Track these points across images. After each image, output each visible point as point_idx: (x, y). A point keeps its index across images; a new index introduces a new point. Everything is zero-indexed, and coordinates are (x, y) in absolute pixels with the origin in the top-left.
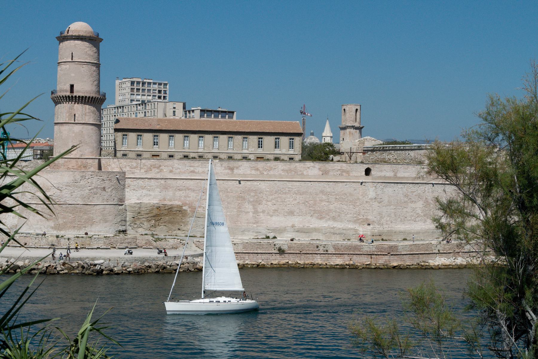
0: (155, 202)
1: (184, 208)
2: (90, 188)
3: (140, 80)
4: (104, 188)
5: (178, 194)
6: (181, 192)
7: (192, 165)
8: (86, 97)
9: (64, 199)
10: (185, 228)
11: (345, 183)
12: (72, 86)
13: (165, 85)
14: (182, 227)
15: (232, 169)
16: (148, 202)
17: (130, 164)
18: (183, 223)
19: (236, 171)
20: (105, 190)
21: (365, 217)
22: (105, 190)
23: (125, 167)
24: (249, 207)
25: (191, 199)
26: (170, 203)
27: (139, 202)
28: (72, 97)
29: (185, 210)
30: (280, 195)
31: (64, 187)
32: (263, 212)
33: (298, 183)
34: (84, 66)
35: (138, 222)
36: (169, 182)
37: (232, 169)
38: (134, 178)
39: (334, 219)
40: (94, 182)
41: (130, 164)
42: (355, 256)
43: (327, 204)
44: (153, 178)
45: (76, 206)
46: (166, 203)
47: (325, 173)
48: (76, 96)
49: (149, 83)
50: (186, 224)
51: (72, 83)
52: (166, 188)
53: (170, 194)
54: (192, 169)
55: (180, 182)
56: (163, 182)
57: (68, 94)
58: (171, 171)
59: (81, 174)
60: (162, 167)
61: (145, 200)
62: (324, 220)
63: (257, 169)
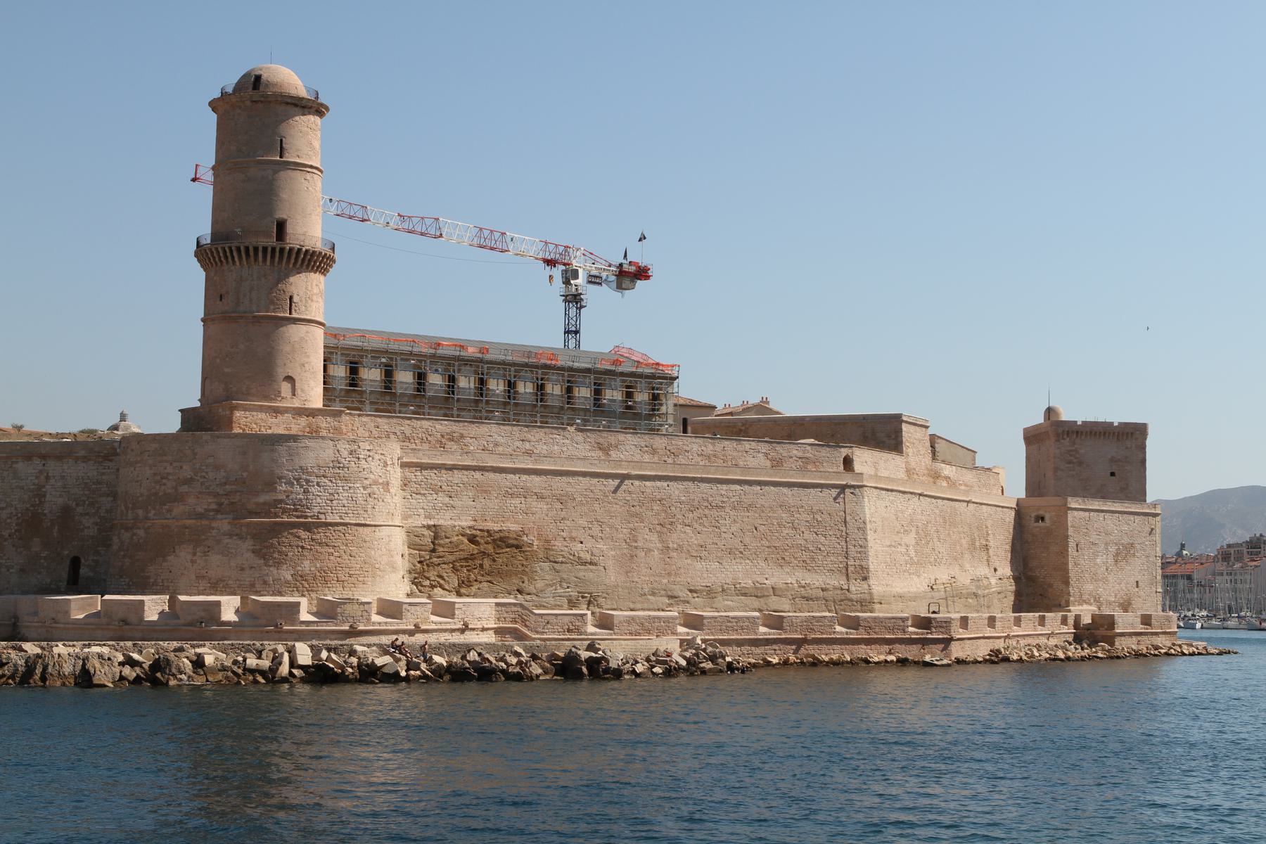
0: (465, 524)
2: (367, 482)
7: (529, 436)
9: (316, 510)
17: (398, 429)
19: (614, 454)
21: (857, 563)
24: (649, 539)
26: (496, 527)
32: (680, 548)
35: (432, 574)
37: (605, 449)
39: (806, 566)
41: (398, 429)
43: (792, 532)
47: (777, 463)
48: (291, 250)
52: (483, 490)
53: (493, 504)
54: (527, 446)
57: (272, 242)
61: (444, 520)
63: (654, 452)
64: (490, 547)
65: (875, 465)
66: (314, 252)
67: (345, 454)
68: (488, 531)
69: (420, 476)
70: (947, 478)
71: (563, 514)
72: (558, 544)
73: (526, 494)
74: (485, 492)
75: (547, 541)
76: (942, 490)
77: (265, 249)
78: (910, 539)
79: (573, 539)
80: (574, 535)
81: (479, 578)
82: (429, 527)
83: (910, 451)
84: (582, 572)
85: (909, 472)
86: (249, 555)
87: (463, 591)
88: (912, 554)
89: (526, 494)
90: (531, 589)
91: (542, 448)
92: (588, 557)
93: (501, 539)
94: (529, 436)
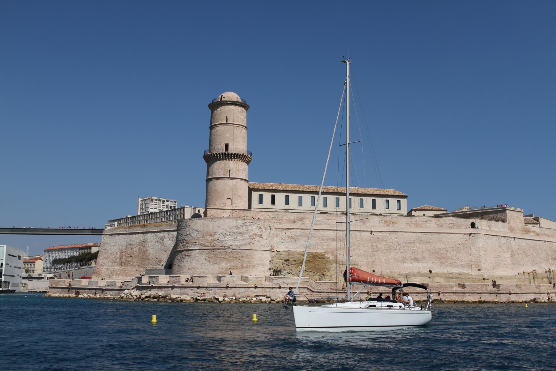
0: (301, 250)
1: (326, 255)
2: (251, 234)
4: (261, 235)
5: (321, 243)
6: (324, 241)
9: (229, 244)
11: (458, 235)
12: (227, 146)
13: (175, 202)
15: (364, 223)
16: (295, 250)
21: (476, 263)
23: (272, 219)
25: (332, 247)
27: (287, 250)
29: (328, 258)
30: (407, 245)
31: (228, 233)
33: (420, 235)
34: (237, 128)
40: (254, 229)
42: (483, 294)
43: (445, 252)
44: (298, 229)
48: (232, 154)
49: (163, 201)
50: (329, 270)
51: (227, 143)
53: (313, 242)
54: (330, 221)
55: (322, 233)
56: (307, 232)
57: (224, 151)
59: (243, 222)
60: (305, 220)
61: (293, 249)
62: (444, 266)
65: (490, 226)
66: (238, 154)
67: (240, 224)
69: (283, 232)
70: (534, 232)
73: (328, 238)
76: (531, 236)
77: (222, 154)
78: (508, 255)
83: (512, 221)
85: (511, 230)
86: (204, 260)
88: (509, 261)
90: (328, 274)
93: (316, 256)
94: (330, 218)
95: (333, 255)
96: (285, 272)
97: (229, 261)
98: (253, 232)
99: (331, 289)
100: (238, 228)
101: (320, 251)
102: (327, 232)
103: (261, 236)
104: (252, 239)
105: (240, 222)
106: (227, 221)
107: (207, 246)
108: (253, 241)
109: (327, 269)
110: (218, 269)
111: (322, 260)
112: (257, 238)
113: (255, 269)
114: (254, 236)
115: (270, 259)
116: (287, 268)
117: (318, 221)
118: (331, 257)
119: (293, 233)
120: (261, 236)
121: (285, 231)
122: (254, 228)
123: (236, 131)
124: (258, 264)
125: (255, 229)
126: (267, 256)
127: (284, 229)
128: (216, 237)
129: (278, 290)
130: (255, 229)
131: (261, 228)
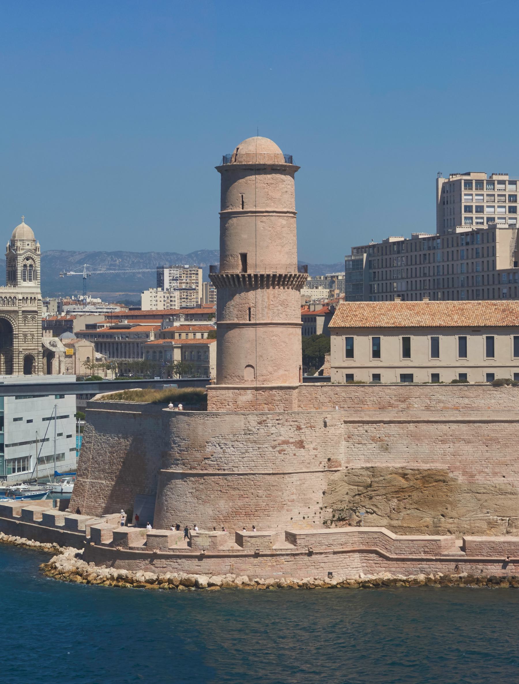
0: (398, 465)
1: (451, 475)
2: (276, 443)
3: (483, 177)
5: (440, 448)
6: (447, 445)
8: (268, 276)
9: (231, 465)
10: (454, 514)
14: (450, 512)
16: (384, 465)
17: (353, 395)
18: (451, 503)
20: (304, 447)
22: (304, 447)
25: (464, 458)
27: (369, 465)
28: (243, 276)
29: (454, 480)
31: (230, 444)
36: (424, 427)
38: (359, 422)
40: (282, 433)
45: (251, 477)
46: (415, 465)
48: (249, 275)
50: (454, 504)
51: (244, 251)
52: (416, 437)
53: (425, 448)
54: (466, 401)
56: (411, 426)
58: (428, 408)
60: (412, 400)
64: (418, 482)
67: (254, 423)
68: (418, 470)
69: (362, 429)
71: (487, 455)
72: (480, 479)
74: (418, 440)
75: (472, 476)
79: (495, 474)
80: (497, 470)
81: (408, 506)
82: (367, 469)
84: (502, 501)
87: (393, 516)
89: (458, 439)
91: (480, 402)
92: (509, 489)
93: (429, 476)
94: (467, 393)
95: (465, 473)
96: (363, 510)
97: (231, 498)
98: (282, 438)
99: (425, 552)
100: (248, 432)
101: (439, 466)
102: (454, 426)
103: (301, 444)
104: (280, 452)
105: (253, 420)
106: (227, 418)
107: (195, 468)
108: (282, 456)
109: (451, 503)
110: (211, 513)
111: (442, 484)
112: (291, 449)
113: (284, 512)
114: (285, 447)
115: (325, 487)
116: (367, 503)
117: (440, 401)
118: (461, 479)
119: (385, 429)
120: (301, 444)
121: (366, 427)
122: (283, 430)
123: (260, 225)
124: (293, 501)
125: (286, 432)
126: (319, 483)
127: (363, 422)
128: (209, 449)
129: (306, 558)
130: (286, 432)
131: (299, 428)
